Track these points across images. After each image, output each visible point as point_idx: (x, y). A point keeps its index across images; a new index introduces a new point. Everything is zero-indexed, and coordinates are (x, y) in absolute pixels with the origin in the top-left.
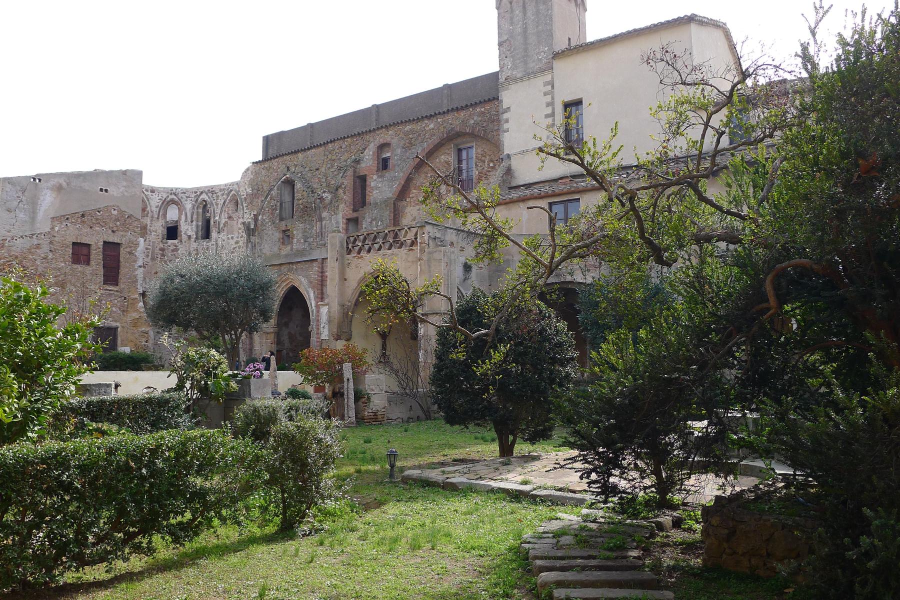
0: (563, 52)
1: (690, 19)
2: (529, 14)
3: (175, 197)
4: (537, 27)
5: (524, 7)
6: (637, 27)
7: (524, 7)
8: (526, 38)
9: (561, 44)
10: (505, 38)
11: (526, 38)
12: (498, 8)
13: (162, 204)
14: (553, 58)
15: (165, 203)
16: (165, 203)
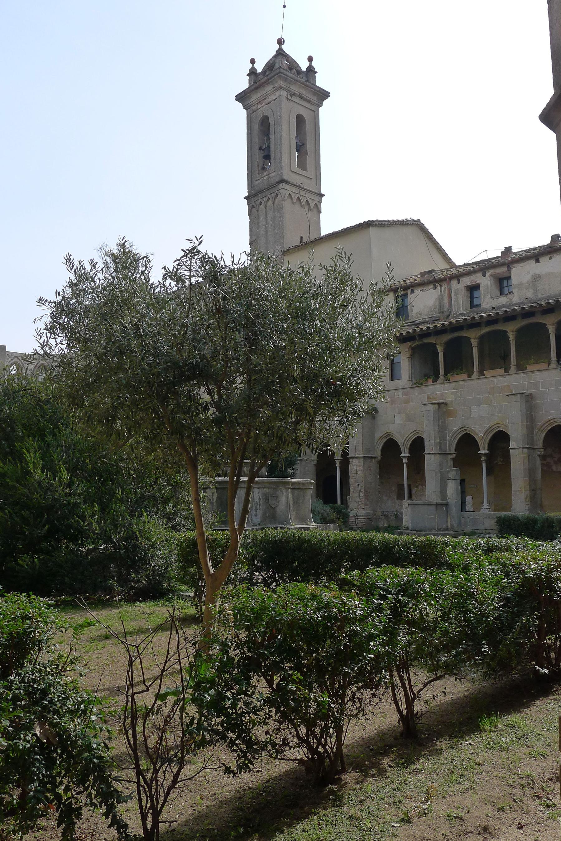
0: (288, 250)
1: (368, 225)
2: (269, 220)
3: (45, 362)
4: (274, 230)
5: (266, 215)
6: (336, 230)
7: (266, 215)
8: (267, 239)
9: (293, 240)
10: (254, 238)
11: (267, 239)
12: (249, 215)
13: (35, 367)
14: (283, 254)
15: (37, 367)
16: (37, 367)
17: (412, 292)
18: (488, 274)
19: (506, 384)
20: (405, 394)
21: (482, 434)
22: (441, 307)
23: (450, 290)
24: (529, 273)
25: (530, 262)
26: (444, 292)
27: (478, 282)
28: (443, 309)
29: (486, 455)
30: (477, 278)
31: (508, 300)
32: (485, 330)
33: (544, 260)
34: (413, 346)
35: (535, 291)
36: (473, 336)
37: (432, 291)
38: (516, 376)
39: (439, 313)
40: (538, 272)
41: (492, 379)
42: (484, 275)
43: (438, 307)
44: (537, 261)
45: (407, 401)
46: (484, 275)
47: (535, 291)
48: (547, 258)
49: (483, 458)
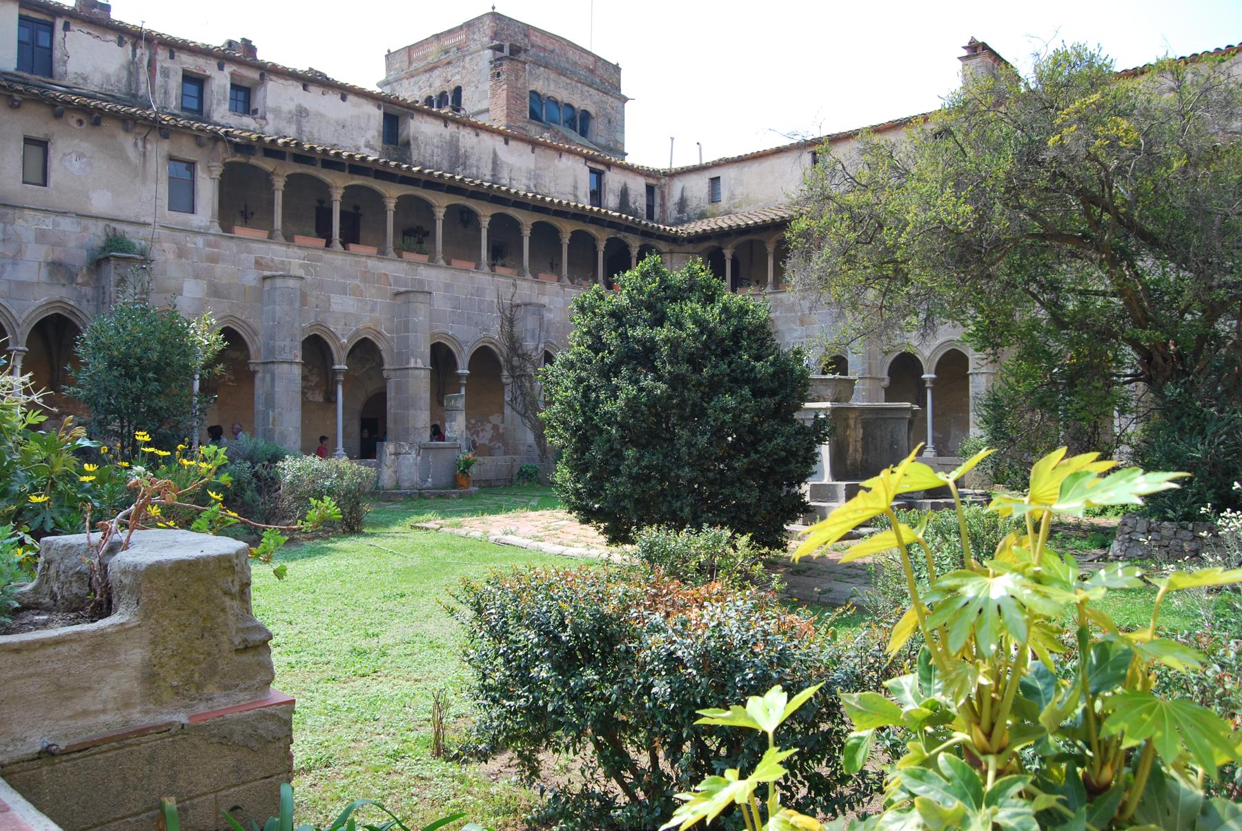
17: (66, 27)
18: (229, 69)
19: (383, 271)
20: (209, 245)
21: (345, 341)
22: (130, 85)
23: (151, 64)
24: (292, 99)
25: (295, 83)
26: (141, 60)
27: (208, 73)
28: (137, 90)
29: (346, 373)
30: (208, 67)
31: (257, 126)
32: (358, 181)
33: (315, 91)
34: (227, 160)
35: (300, 130)
36: (392, 193)
37: (114, 46)
38: (397, 263)
39: (127, 94)
40: (306, 105)
41: (364, 259)
42: (221, 68)
43: (124, 81)
44: (305, 88)
45: (214, 259)
46: (221, 68)
47: (300, 130)
48: (319, 90)
49: (341, 378)
